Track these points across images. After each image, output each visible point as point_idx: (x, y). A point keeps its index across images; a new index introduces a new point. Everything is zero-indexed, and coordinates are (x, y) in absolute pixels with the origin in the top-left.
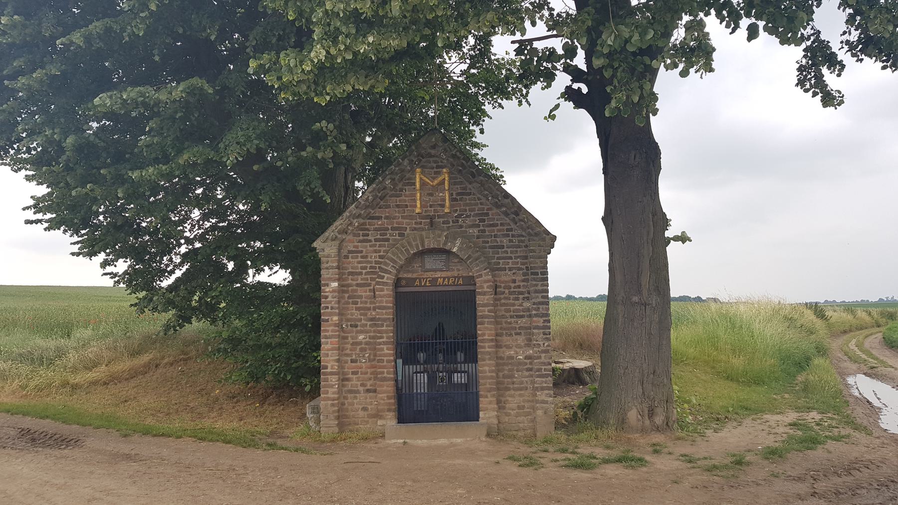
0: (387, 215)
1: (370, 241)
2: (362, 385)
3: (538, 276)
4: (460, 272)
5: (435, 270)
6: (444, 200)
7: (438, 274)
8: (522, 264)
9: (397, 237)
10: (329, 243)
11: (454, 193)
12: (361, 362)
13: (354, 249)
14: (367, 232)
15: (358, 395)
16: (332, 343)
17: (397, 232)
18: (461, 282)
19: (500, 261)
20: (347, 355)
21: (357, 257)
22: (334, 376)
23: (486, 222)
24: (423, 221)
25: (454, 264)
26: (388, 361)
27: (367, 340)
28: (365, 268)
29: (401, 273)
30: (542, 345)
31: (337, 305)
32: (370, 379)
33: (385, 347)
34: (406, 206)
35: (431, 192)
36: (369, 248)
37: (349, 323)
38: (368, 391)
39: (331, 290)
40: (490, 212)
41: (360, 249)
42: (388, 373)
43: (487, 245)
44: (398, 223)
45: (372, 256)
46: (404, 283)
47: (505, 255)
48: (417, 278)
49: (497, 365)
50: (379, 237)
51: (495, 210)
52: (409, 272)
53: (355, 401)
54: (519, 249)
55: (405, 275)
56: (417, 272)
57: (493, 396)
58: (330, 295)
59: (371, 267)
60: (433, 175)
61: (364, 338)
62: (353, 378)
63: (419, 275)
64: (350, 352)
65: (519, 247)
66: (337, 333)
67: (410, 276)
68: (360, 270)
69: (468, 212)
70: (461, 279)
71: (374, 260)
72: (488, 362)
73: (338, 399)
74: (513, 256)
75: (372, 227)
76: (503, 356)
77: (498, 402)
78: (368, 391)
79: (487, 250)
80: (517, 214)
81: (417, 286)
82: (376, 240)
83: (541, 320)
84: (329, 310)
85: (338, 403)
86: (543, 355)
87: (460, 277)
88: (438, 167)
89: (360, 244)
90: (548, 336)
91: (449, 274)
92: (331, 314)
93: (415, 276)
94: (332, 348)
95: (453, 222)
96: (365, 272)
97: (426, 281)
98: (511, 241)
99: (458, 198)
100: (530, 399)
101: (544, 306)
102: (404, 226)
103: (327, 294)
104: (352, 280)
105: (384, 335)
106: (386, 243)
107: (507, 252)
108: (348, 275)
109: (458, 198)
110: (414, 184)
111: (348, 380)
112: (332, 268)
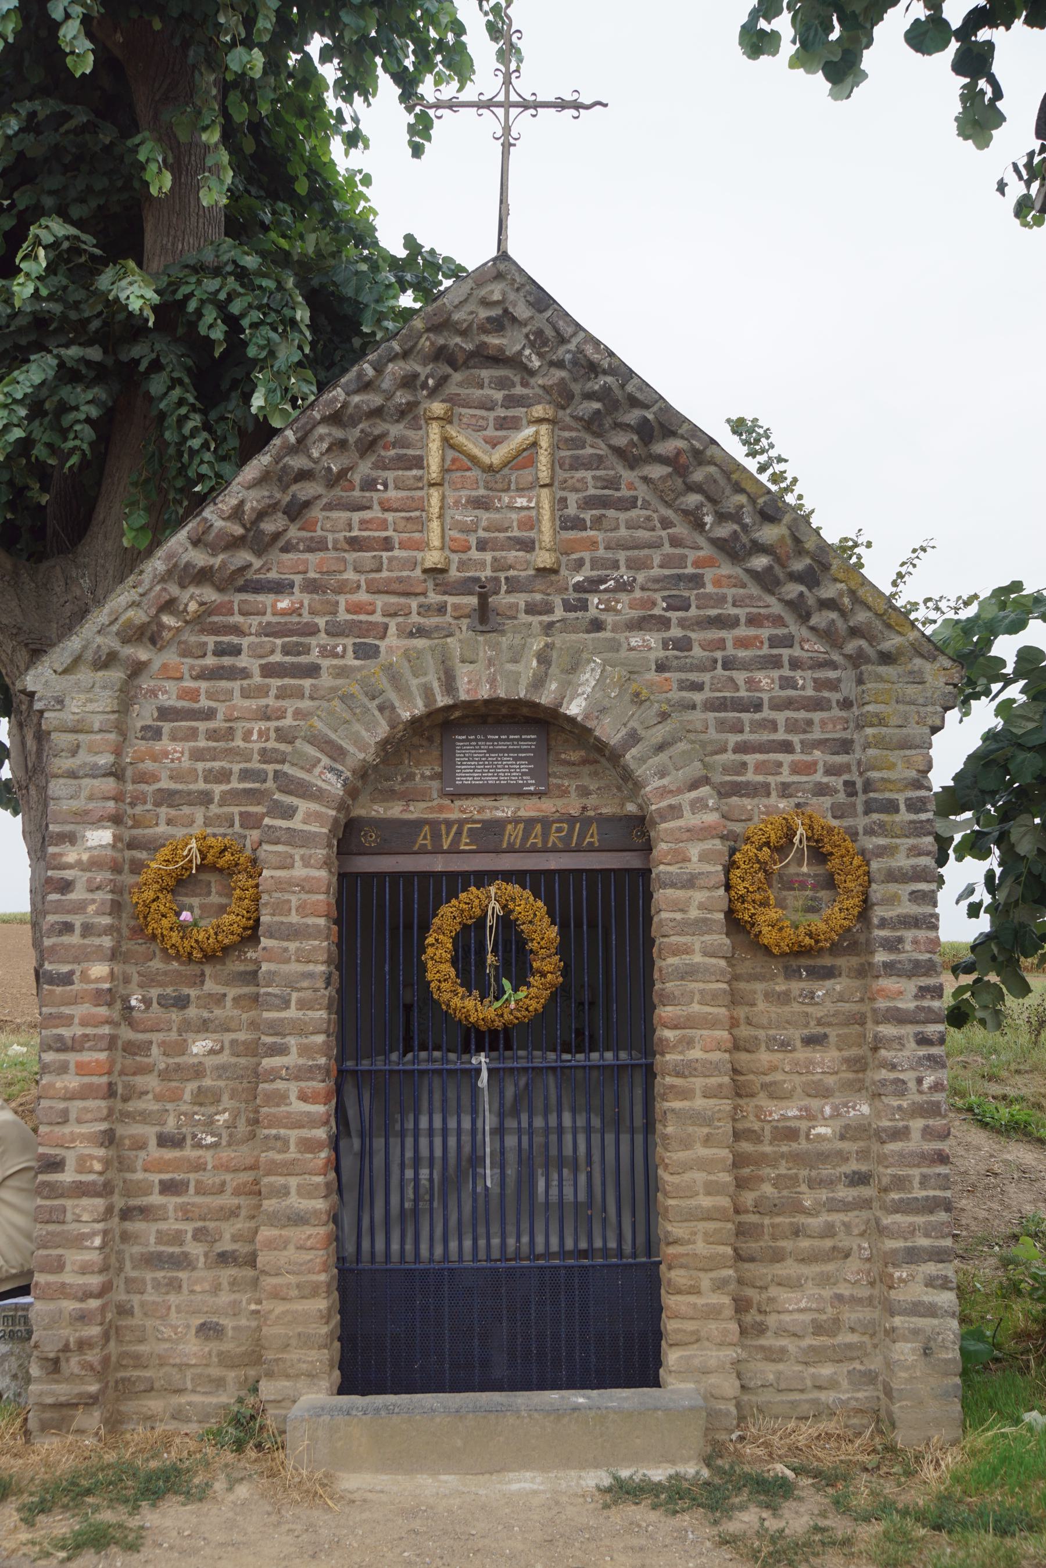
0: (312, 575)
1: (244, 674)
2: (199, 1235)
3: (897, 818)
4: (592, 801)
5: (495, 793)
6: (531, 524)
7: (505, 809)
8: (830, 771)
9: (351, 661)
10: (85, 675)
11: (573, 498)
12: (199, 1145)
13: (180, 704)
14: (236, 640)
15: (181, 1275)
16: (82, 1069)
17: (349, 641)
18: (593, 837)
19: (747, 758)
20: (144, 1117)
21: (193, 734)
22: (85, 1201)
23: (693, 611)
24: (451, 600)
26: (308, 1146)
27: (225, 1058)
28: (224, 776)
29: (364, 798)
30: (912, 1085)
31: (106, 920)
32: (233, 1213)
33: (293, 1088)
34: (387, 544)
35: (482, 492)
36: (238, 701)
37: (154, 993)
38: (224, 1258)
39: (85, 857)
40: (709, 574)
41: (204, 703)
42: (305, 1192)
43: (698, 697)
44: (355, 609)
45: (250, 732)
46: (371, 839)
47: (766, 736)
48: (426, 822)
49: (739, 1161)
50: (277, 658)
51: (726, 569)
52: (390, 795)
53: (173, 1299)
54: (817, 716)
55: (379, 810)
56: (422, 796)
57: (720, 1286)
58: (81, 878)
59: (246, 775)
60: (491, 432)
61: (212, 1052)
62: (163, 1207)
63: (431, 809)
64: (155, 1107)
65: (818, 705)
66: (106, 1030)
67: (395, 811)
68: (201, 785)
69: (623, 569)
71: (257, 746)
72: (703, 1152)
73: (105, 1290)
74: (795, 739)
75: (255, 621)
76: (756, 1126)
77: (741, 1306)
78: (224, 1258)
79: (697, 716)
80: (810, 578)
81: (423, 851)
82: (268, 671)
83: (910, 986)
84: (74, 939)
85: (103, 1309)
86: (917, 1125)
88: (511, 401)
89: (203, 685)
90: (935, 1050)
91: (547, 806)
92: (83, 956)
93: (416, 811)
94: (83, 1086)
95: (568, 607)
96: (224, 793)
97: (459, 833)
98: (787, 683)
99: (587, 516)
100: (864, 1292)
101: (922, 934)
102: (377, 617)
103: (68, 874)
104: (169, 822)
105: (292, 1041)
106: (307, 683)
107: (773, 726)
108: (157, 804)
109: (587, 516)
110: (418, 462)
111: (145, 1212)
112: (95, 773)
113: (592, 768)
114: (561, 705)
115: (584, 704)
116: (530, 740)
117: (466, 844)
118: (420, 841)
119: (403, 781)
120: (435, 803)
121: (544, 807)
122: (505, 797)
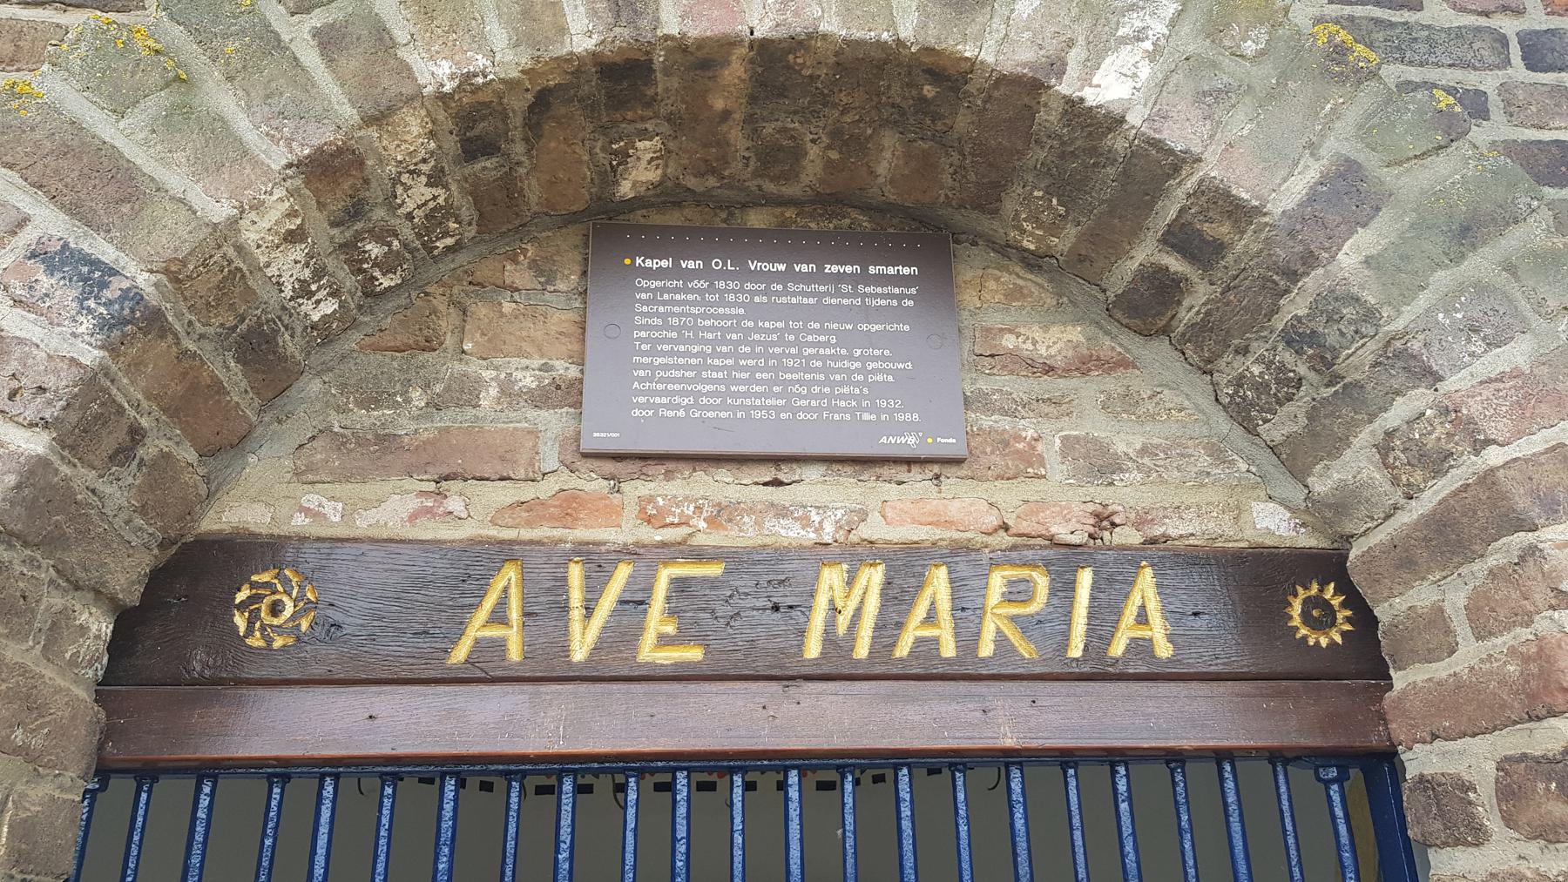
4: (1126, 494)
25: (1020, 386)
48: (505, 552)
70: (1147, 578)
87: (1131, 559)
97: (634, 603)
113: (1114, 384)
114: (1057, 67)
115: (1145, 71)
116: (898, 280)
117: (664, 641)
118: (477, 628)
119: (435, 405)
120: (546, 489)
121: (954, 509)
122: (813, 473)
